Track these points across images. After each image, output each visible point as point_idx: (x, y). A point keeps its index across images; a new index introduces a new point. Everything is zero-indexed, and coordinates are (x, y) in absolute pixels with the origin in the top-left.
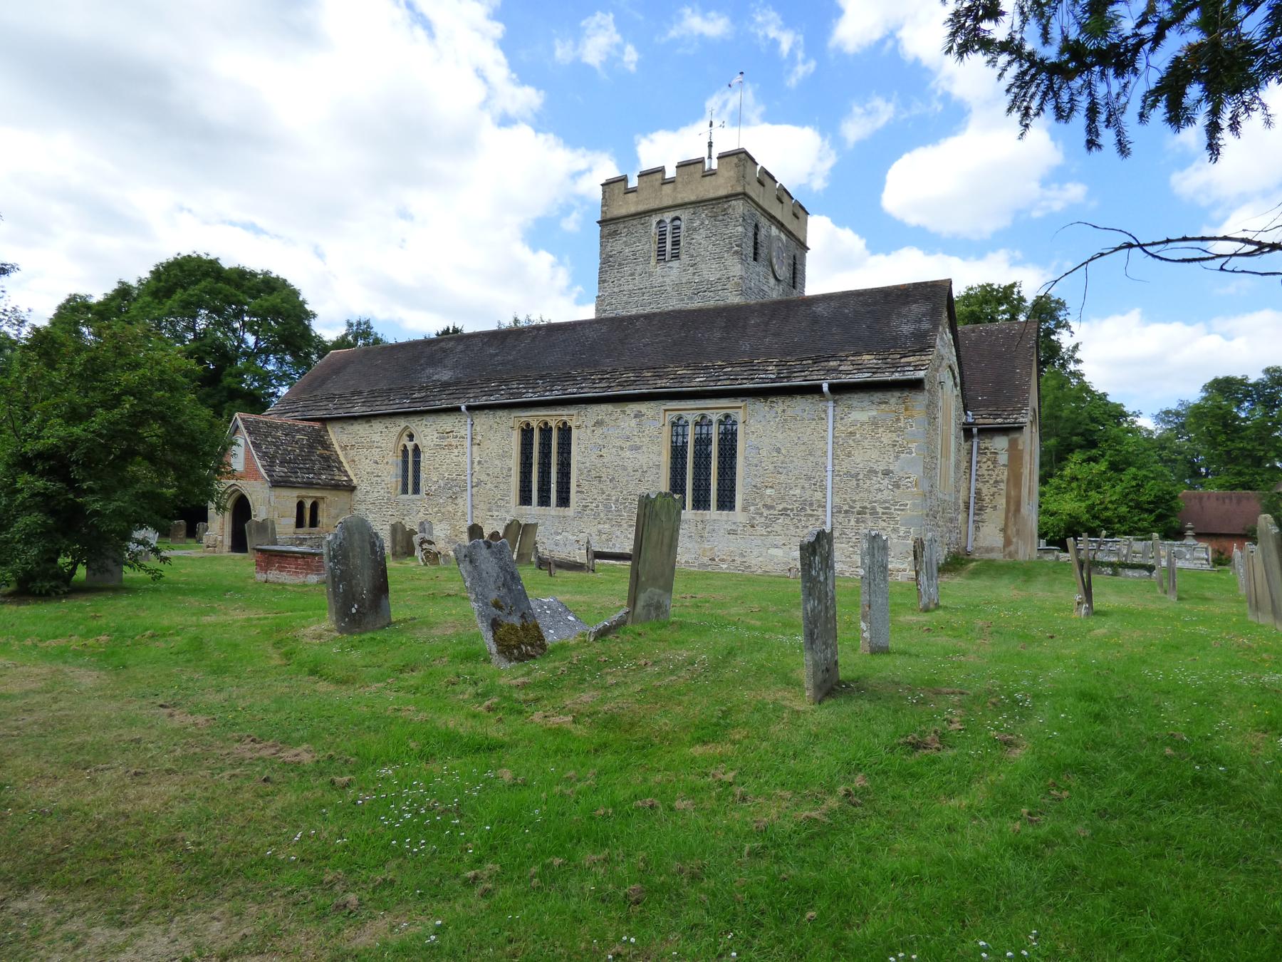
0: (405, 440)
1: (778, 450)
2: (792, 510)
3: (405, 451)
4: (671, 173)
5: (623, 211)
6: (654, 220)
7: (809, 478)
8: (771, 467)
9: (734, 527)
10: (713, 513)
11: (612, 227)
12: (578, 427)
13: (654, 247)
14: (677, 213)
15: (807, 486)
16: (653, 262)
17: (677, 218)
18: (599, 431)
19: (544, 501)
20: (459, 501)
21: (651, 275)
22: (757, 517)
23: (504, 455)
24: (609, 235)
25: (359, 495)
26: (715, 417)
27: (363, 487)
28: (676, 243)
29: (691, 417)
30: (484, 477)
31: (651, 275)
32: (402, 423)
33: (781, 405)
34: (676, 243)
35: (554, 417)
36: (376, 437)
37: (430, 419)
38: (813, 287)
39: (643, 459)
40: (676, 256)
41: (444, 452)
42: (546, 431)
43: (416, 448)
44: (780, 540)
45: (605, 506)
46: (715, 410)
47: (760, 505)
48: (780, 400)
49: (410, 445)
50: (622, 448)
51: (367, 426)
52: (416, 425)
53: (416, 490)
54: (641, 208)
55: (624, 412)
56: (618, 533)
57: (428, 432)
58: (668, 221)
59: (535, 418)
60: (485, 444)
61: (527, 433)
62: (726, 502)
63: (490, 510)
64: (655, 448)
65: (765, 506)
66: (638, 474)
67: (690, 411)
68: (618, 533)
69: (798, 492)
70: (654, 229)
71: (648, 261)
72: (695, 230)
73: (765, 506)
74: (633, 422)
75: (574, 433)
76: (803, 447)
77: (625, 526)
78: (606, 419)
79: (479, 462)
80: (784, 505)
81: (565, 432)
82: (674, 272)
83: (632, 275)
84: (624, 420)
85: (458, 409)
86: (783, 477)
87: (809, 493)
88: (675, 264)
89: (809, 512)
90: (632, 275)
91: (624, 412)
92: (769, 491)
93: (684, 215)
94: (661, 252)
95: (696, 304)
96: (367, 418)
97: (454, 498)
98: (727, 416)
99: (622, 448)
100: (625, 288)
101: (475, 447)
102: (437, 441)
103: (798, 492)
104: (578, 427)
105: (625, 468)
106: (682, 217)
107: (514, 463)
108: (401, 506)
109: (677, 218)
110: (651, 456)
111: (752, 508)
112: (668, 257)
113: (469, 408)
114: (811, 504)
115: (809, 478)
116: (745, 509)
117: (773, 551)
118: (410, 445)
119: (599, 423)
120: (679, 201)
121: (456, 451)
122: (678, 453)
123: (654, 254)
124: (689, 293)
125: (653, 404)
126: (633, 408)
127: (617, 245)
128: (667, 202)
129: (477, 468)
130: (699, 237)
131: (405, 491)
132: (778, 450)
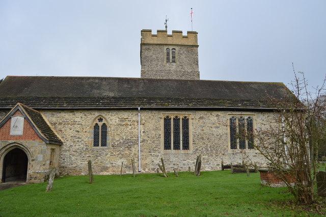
0: (97, 121)
3: (96, 126)
4: (170, 33)
5: (152, 42)
6: (165, 48)
12: (192, 119)
13: (166, 57)
14: (174, 47)
17: (174, 49)
19: (177, 147)
20: (133, 149)
21: (165, 66)
23: (157, 129)
25: (64, 147)
26: (181, 117)
27: (67, 144)
30: (146, 138)
32: (97, 114)
34: (174, 57)
35: (181, 115)
36: (76, 119)
37: (114, 113)
38: (202, 78)
39: (220, 131)
40: (174, 62)
41: (123, 127)
42: (176, 120)
43: (104, 126)
45: (206, 149)
46: (246, 116)
49: (100, 124)
50: (211, 127)
51: (71, 114)
52: (104, 114)
53: (104, 144)
54: (159, 43)
55: (212, 114)
56: (212, 159)
57: (112, 119)
58: (171, 49)
59: (172, 115)
60: (147, 124)
61: (167, 120)
63: (150, 152)
67: (237, 115)
68: (212, 159)
70: (165, 51)
71: (163, 61)
72: (181, 54)
74: (216, 118)
75: (190, 121)
79: (144, 132)
81: (186, 121)
82: (174, 67)
84: (212, 118)
85: (137, 109)
88: (174, 64)
91: (212, 114)
93: (177, 48)
94: (168, 59)
95: (183, 78)
96: (72, 110)
97: (129, 148)
98: (249, 117)
99: (211, 127)
101: (142, 126)
102: (119, 123)
104: (192, 119)
105: (213, 135)
107: (162, 132)
108: (95, 152)
109: (174, 49)
112: (171, 61)
113: (141, 109)
118: (100, 124)
119: (201, 118)
120: (174, 43)
121: (130, 127)
122: (233, 130)
123: (165, 59)
125: (223, 112)
127: (146, 53)
128: (170, 42)
129: (143, 134)
130: (183, 57)
131: (96, 144)
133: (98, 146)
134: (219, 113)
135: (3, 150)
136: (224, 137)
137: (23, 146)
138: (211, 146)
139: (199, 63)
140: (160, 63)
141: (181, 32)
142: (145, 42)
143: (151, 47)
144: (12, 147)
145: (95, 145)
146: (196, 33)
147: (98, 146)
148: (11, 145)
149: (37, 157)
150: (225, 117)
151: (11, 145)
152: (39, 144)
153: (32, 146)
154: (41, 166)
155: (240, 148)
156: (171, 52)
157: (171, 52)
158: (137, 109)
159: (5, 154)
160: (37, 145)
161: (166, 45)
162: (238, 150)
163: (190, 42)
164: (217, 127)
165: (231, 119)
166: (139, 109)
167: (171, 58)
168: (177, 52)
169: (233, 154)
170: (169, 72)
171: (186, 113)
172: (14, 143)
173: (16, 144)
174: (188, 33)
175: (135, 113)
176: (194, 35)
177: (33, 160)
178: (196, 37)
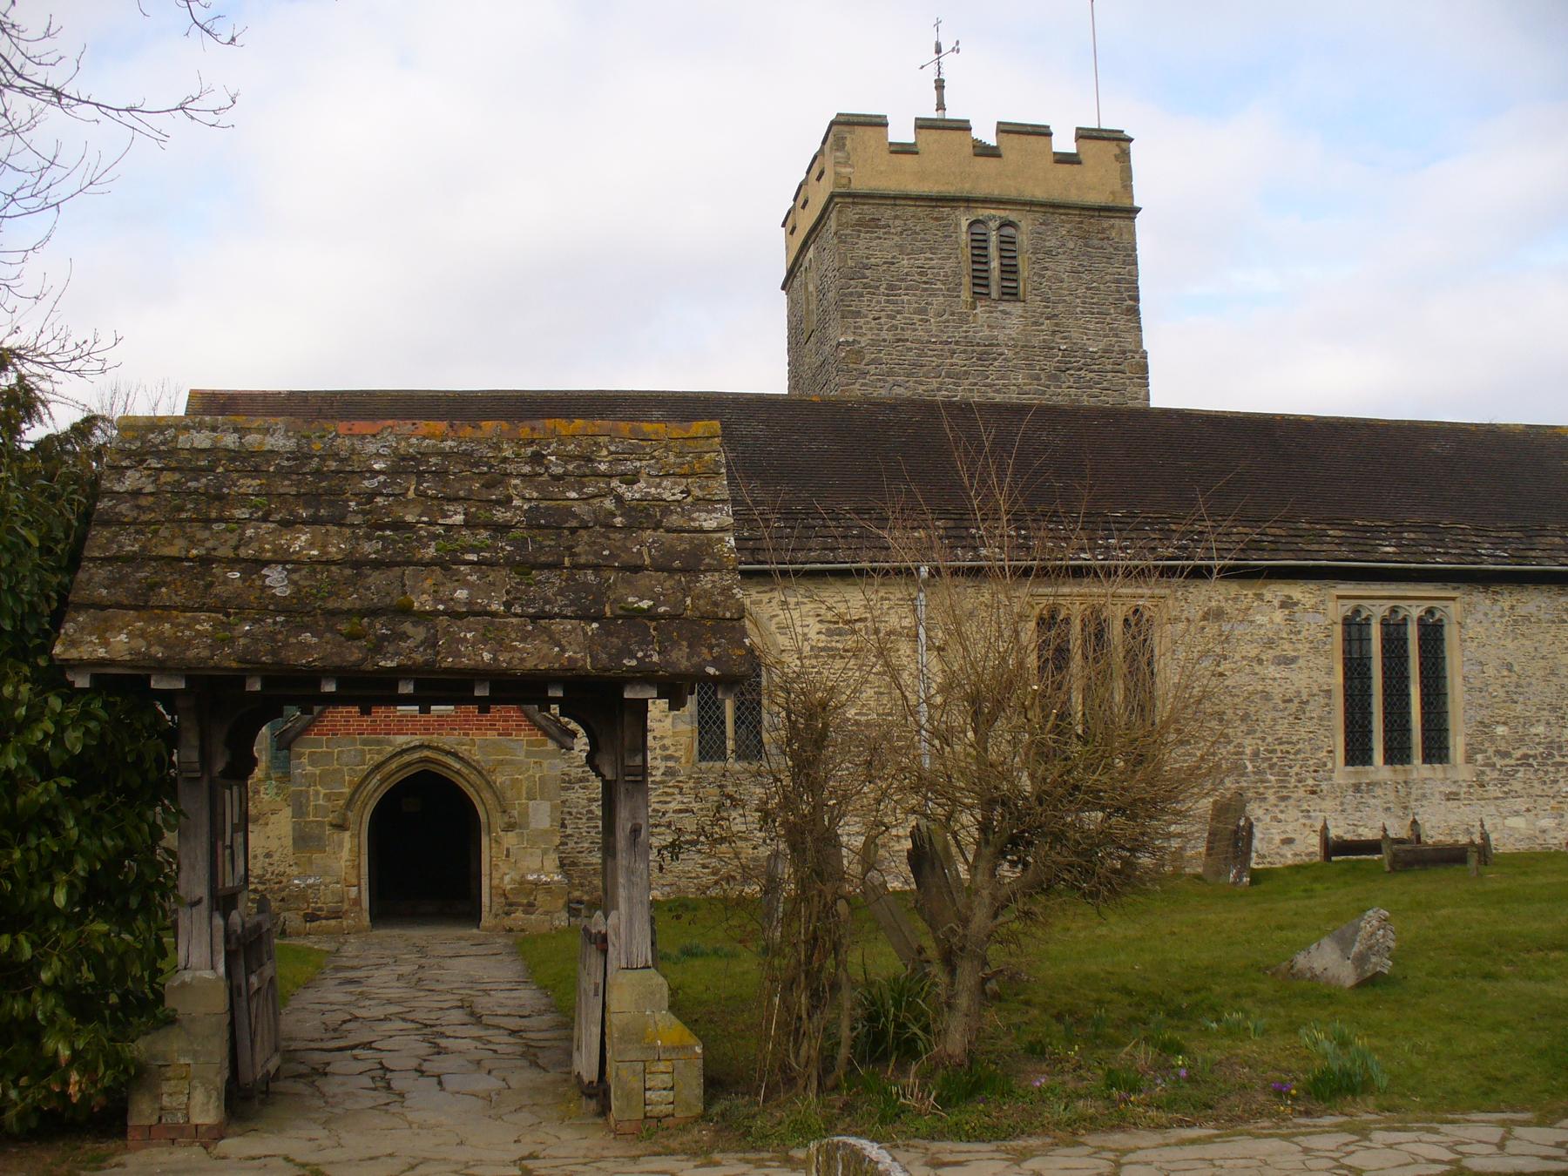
1: (1510, 667)
2: (1535, 757)
7: (1554, 709)
8: (1501, 693)
9: (1454, 789)
10: (1418, 768)
11: (869, 210)
13: (966, 267)
15: (1552, 720)
16: (966, 295)
18: (1211, 629)
22: (1487, 770)
24: (860, 223)
28: (1009, 270)
29: (1379, 610)
31: (963, 319)
33: (1507, 599)
34: (1009, 270)
39: (1300, 680)
40: (1011, 294)
44: (1520, 804)
46: (1414, 602)
47: (1490, 752)
48: (1505, 589)
50: (1260, 662)
55: (1259, 597)
58: (993, 225)
62: (1436, 750)
64: (1322, 661)
65: (1497, 752)
66: (1293, 707)
68: (1260, 812)
69: (1540, 729)
71: (953, 291)
72: (1048, 252)
73: (1497, 752)
74: (1279, 616)
76: (1543, 663)
77: (1272, 799)
78: (1228, 607)
80: (1524, 750)
83: (922, 311)
86: (1519, 707)
87: (1556, 730)
88: (1016, 308)
89: (1558, 759)
90: (922, 311)
91: (1259, 597)
92: (1501, 730)
93: (1027, 225)
94: (980, 281)
95: (1063, 394)
98: (1430, 611)
100: (908, 334)
103: (1540, 729)
105: (1267, 696)
106: (1023, 224)
109: (1006, 224)
110: (1315, 674)
111: (1479, 757)
113: (935, 572)
114: (1560, 748)
115: (1554, 709)
116: (1469, 759)
117: (1513, 822)
119: (1218, 615)
122: (1356, 670)
124: (1050, 366)
125: (1312, 586)
126: (1276, 591)
132: (1510, 667)
133: (723, 756)
134: (1297, 591)
135: (375, 781)
136: (1314, 710)
137: (461, 759)
138: (1256, 754)
139: (1143, 306)
140: (937, 302)
141: (1044, 132)
142: (858, 185)
143: (889, 213)
144: (409, 764)
145: (703, 756)
146: (1119, 140)
147: (723, 756)
148: (406, 758)
149: (525, 813)
150: (1321, 609)
151: (406, 758)
152: (528, 754)
153: (501, 762)
154: (545, 852)
155: (1389, 759)
156: (994, 238)
157: (994, 238)
158: (909, 573)
159: (378, 795)
160: (521, 757)
161: (969, 201)
162: (1378, 768)
163: (1090, 187)
164: (1286, 661)
165: (1348, 622)
166: (924, 571)
167: (994, 276)
168: (1024, 239)
169: (1357, 788)
170: (985, 353)
171: (1146, 591)
172: (422, 747)
173: (427, 753)
174: (1083, 135)
175: (898, 592)
176: (1112, 148)
177: (510, 827)
178: (1124, 157)
